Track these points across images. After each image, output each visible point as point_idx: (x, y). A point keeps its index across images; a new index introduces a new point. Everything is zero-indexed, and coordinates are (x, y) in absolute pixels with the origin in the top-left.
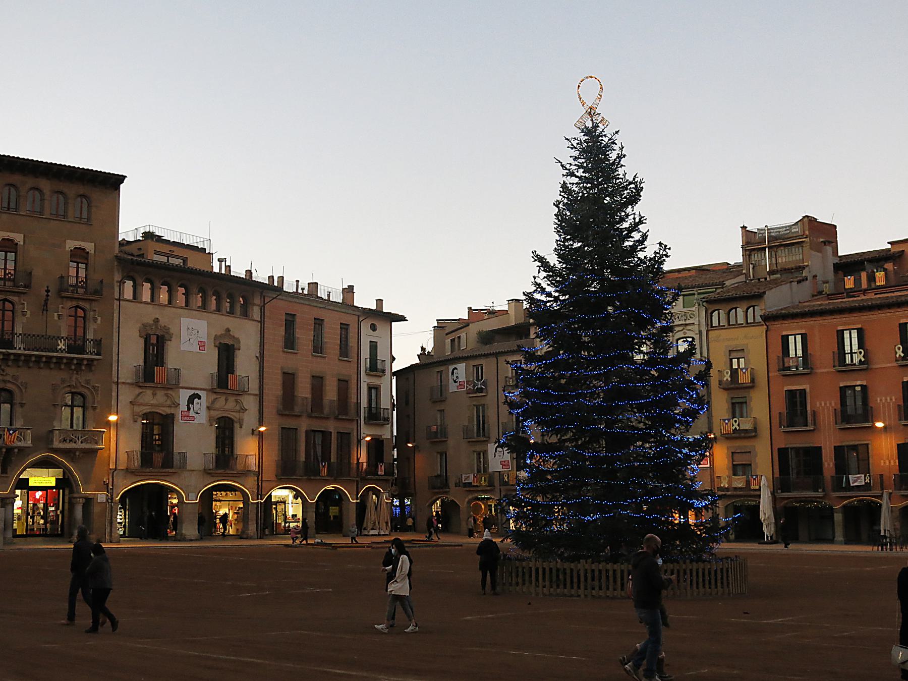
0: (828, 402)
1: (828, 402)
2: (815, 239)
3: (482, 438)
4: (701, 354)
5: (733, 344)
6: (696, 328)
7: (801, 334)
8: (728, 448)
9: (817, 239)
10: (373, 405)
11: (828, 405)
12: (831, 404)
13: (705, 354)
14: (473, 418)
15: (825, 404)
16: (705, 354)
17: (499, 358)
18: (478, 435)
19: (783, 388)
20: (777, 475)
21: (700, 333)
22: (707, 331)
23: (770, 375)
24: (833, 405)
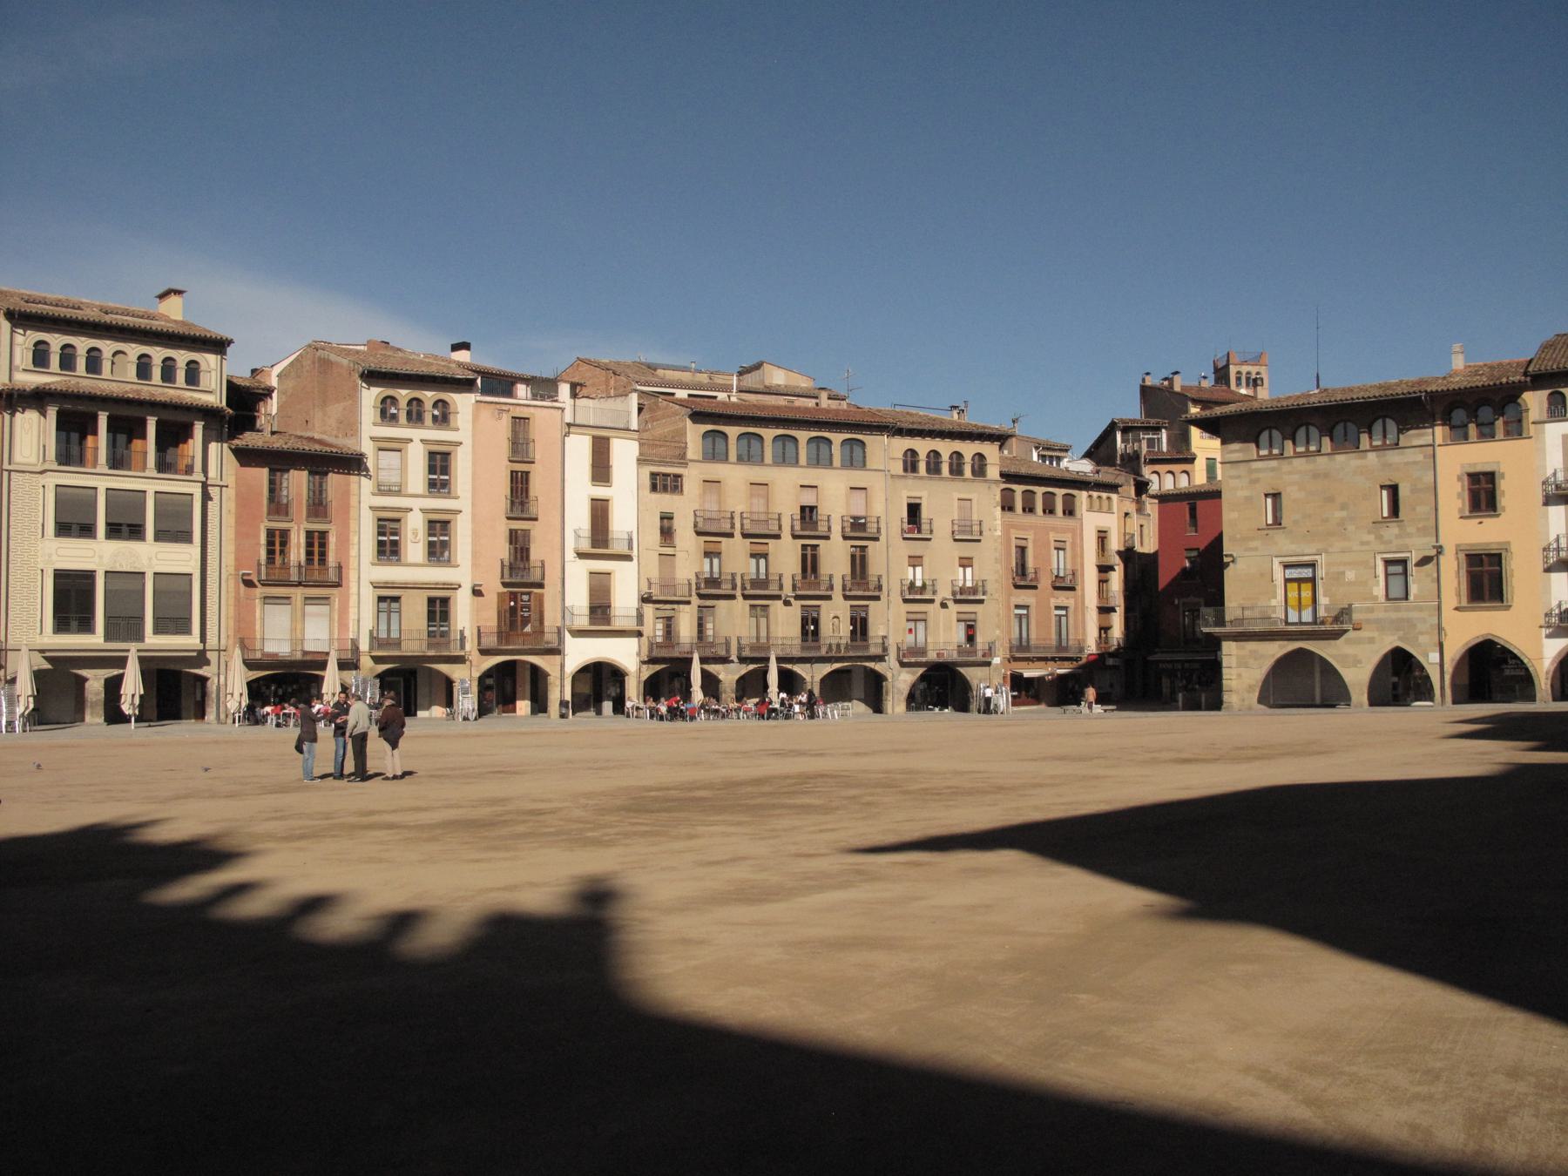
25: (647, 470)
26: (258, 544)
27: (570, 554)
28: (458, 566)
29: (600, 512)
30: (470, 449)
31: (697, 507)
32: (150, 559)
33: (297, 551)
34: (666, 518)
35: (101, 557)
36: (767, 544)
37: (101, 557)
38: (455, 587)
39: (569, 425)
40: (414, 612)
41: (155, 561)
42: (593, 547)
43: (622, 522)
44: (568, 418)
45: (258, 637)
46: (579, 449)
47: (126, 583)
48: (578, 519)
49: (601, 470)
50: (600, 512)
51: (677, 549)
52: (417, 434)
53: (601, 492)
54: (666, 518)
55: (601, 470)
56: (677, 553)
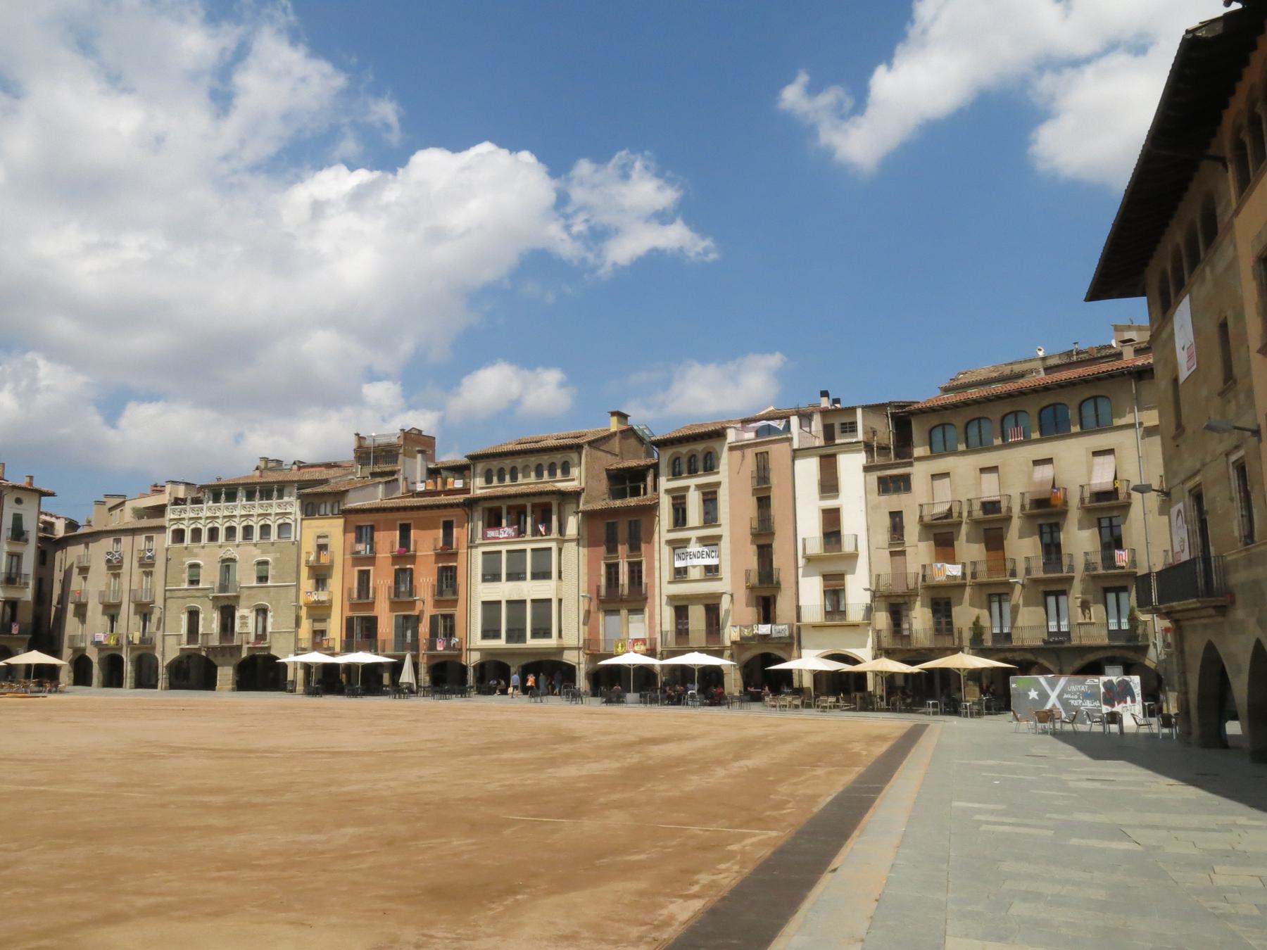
2: (410, 448)
4: (295, 537)
5: (320, 531)
9: (412, 448)
10: (14, 570)
12: (387, 582)
13: (298, 538)
15: (384, 582)
16: (298, 538)
20: (344, 638)
22: (302, 520)
25: (873, 477)
26: (600, 575)
27: (801, 562)
28: (721, 579)
29: (832, 519)
30: (727, 485)
31: (924, 500)
32: (529, 592)
33: (624, 578)
34: (896, 517)
35: (503, 592)
36: (804, 540)
37: (503, 592)
38: (719, 596)
39: (795, 451)
40: (697, 617)
41: (531, 592)
42: (825, 552)
43: (854, 524)
44: (796, 445)
45: (601, 637)
46: (808, 469)
47: (516, 605)
48: (810, 528)
49: (829, 485)
50: (832, 519)
51: (907, 544)
52: (692, 482)
53: (830, 504)
54: (896, 517)
55: (829, 485)
56: (907, 549)
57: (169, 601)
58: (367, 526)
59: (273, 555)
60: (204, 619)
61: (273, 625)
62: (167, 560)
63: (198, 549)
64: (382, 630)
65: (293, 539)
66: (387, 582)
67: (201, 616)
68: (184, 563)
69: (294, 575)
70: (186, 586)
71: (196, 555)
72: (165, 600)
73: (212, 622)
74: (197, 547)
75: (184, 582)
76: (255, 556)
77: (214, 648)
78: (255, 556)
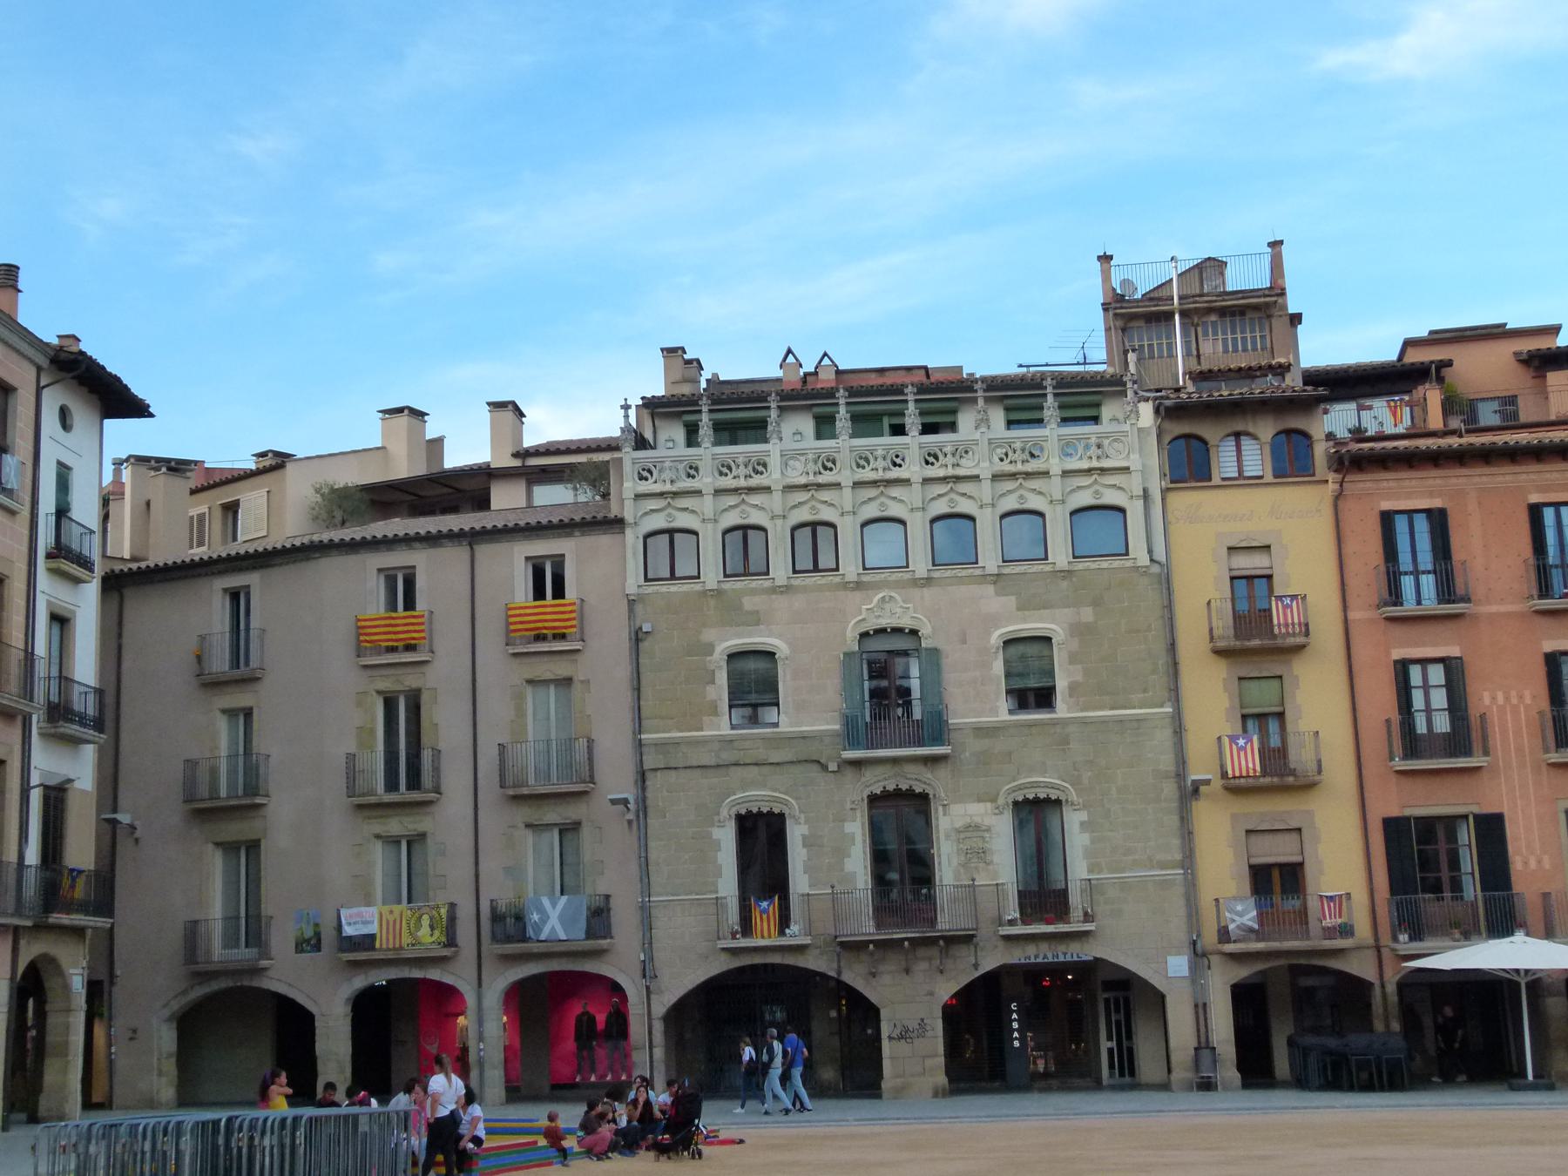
0: (1513, 693)
1: (1513, 693)
3: (404, 794)
5: (1241, 532)
6: (1135, 484)
7: (1428, 512)
8: (1234, 817)
11: (1514, 701)
12: (1521, 697)
13: (1160, 554)
14: (372, 731)
15: (1507, 699)
17: (475, 547)
18: (392, 785)
19: (1388, 654)
21: (1146, 495)
23: (1352, 615)
24: (1528, 701)
57: (654, 782)
58: (1410, 513)
59: (1067, 614)
60: (807, 842)
61: (1088, 853)
62: (638, 637)
63: (757, 599)
64: (1526, 863)
65: (1144, 560)
66: (1521, 697)
67: (795, 834)
68: (709, 649)
69: (1159, 681)
70: (721, 726)
71: (755, 620)
72: (642, 776)
73: (841, 853)
74: (754, 592)
75: (714, 711)
76: (992, 621)
77: (854, 948)
78: (992, 621)
